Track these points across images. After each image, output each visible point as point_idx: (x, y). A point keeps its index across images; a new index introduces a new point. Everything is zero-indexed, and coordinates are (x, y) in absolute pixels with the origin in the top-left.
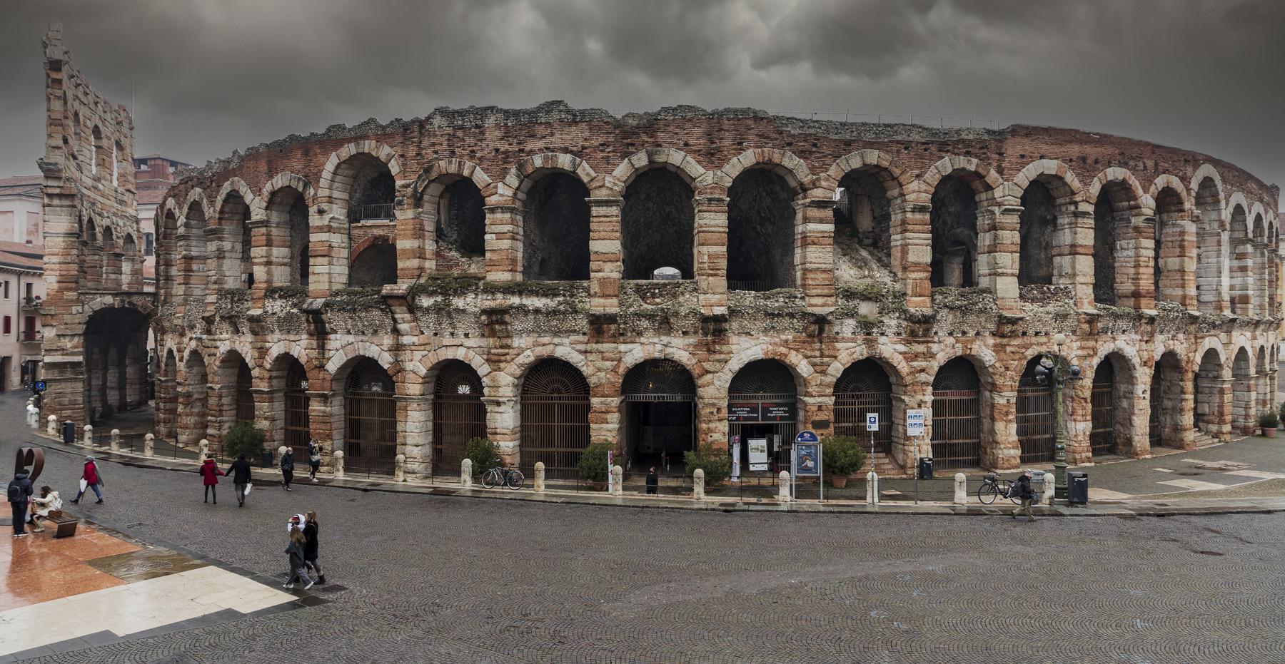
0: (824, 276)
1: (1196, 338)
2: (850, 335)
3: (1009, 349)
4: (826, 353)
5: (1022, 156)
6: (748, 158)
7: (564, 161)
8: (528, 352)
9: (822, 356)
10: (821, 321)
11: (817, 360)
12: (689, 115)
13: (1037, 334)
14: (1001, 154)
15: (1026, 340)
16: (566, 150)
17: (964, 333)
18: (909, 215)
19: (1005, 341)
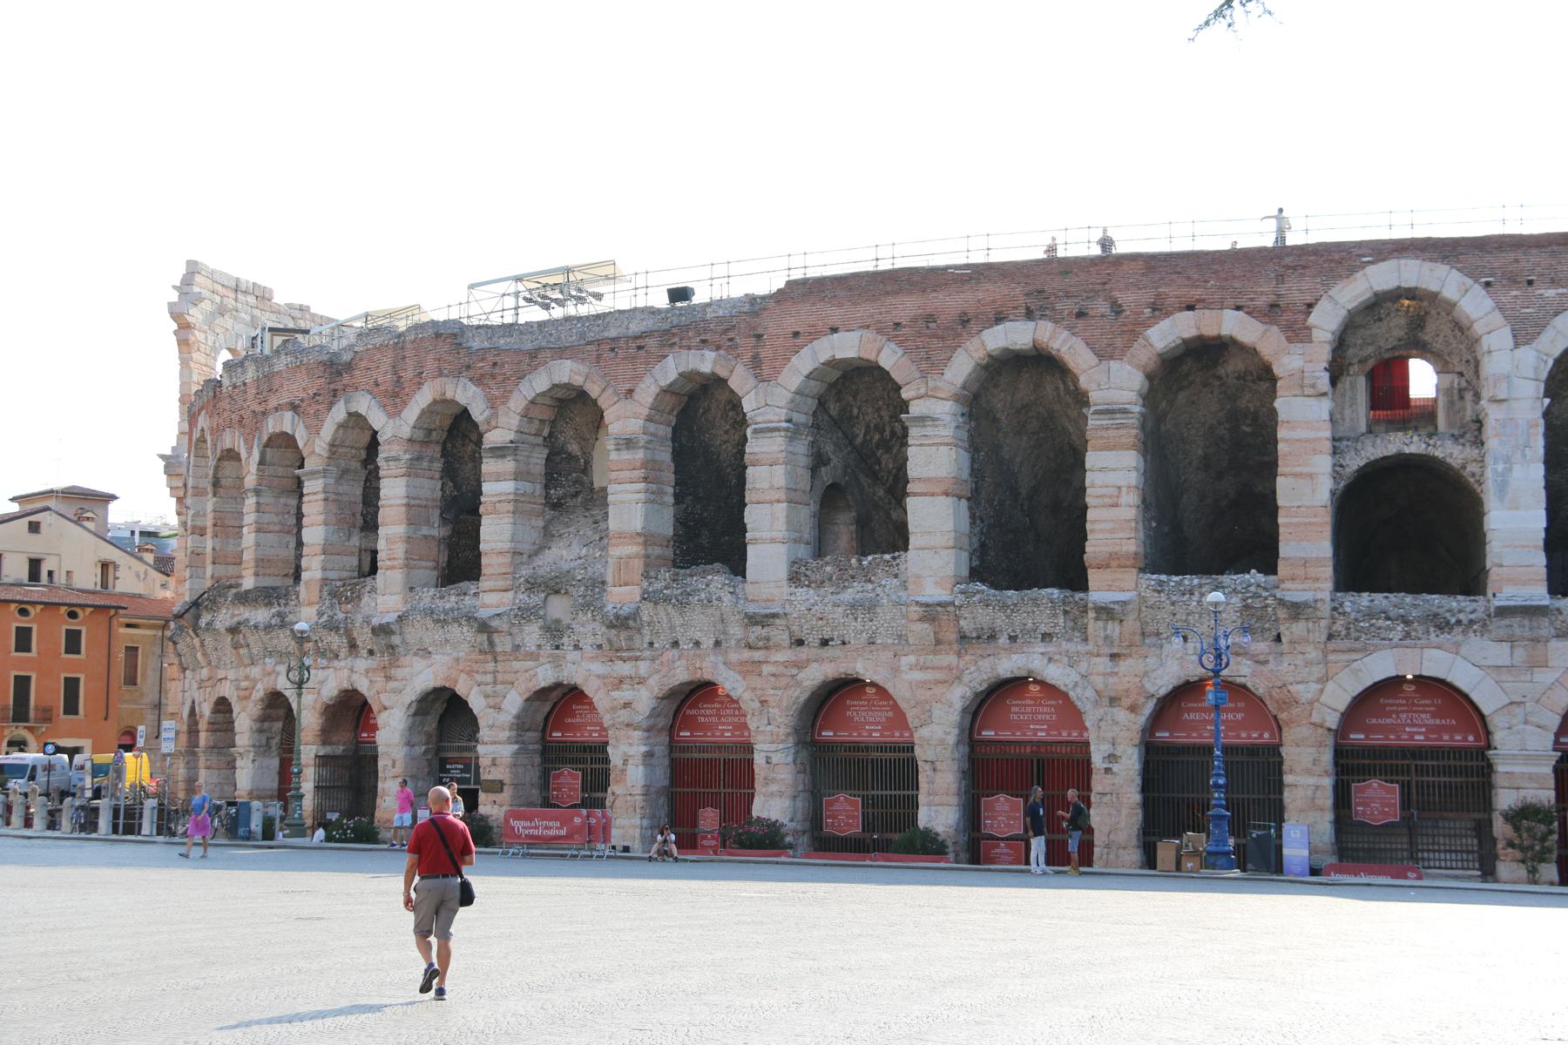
0: (501, 559)
1: (1325, 653)
2: (534, 648)
3: (766, 669)
4: (500, 677)
5: (796, 334)
6: (423, 399)
7: (286, 422)
8: (259, 686)
9: (495, 683)
10: (484, 627)
11: (489, 689)
12: (378, 341)
13: (825, 643)
14: (759, 337)
15: (803, 653)
16: (294, 407)
17: (697, 644)
18: (614, 456)
19: (758, 655)
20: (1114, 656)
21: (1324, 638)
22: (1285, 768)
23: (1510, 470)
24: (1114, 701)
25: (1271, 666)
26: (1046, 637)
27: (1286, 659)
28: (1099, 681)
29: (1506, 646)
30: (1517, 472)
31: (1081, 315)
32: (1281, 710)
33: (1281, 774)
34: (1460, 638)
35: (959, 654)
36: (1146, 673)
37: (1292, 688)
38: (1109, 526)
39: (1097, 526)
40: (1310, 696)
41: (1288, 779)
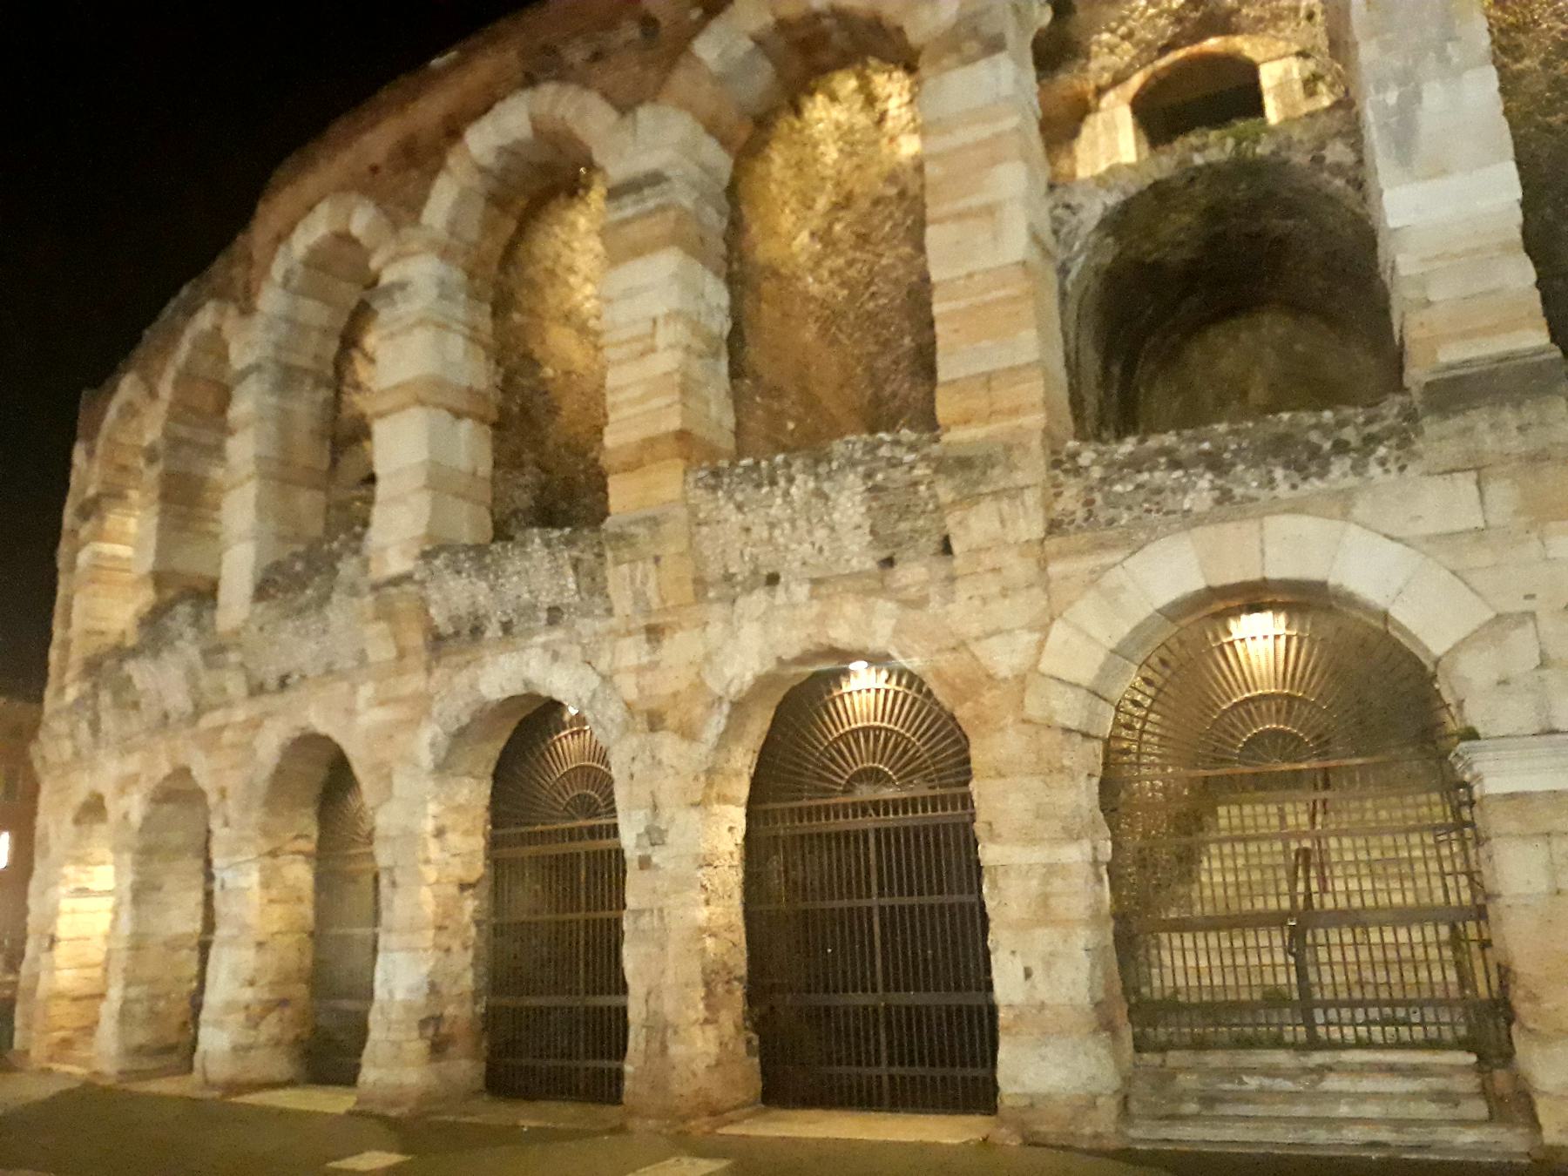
3: (228, 736)
13: (283, 683)
20: (654, 633)
21: (1037, 529)
22: (979, 828)
23: (1417, 96)
24: (655, 722)
25: (934, 606)
26: (555, 615)
27: (963, 590)
28: (628, 687)
29: (1465, 484)
30: (1434, 96)
31: (597, 56)
32: (962, 698)
33: (972, 843)
34: (1352, 481)
35: (429, 671)
36: (708, 658)
37: (976, 649)
38: (637, 392)
39: (622, 397)
40: (1016, 660)
41: (989, 854)
